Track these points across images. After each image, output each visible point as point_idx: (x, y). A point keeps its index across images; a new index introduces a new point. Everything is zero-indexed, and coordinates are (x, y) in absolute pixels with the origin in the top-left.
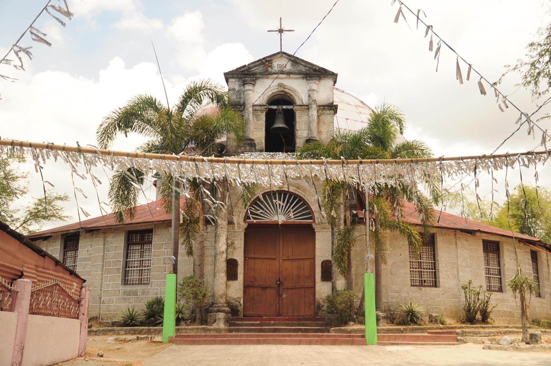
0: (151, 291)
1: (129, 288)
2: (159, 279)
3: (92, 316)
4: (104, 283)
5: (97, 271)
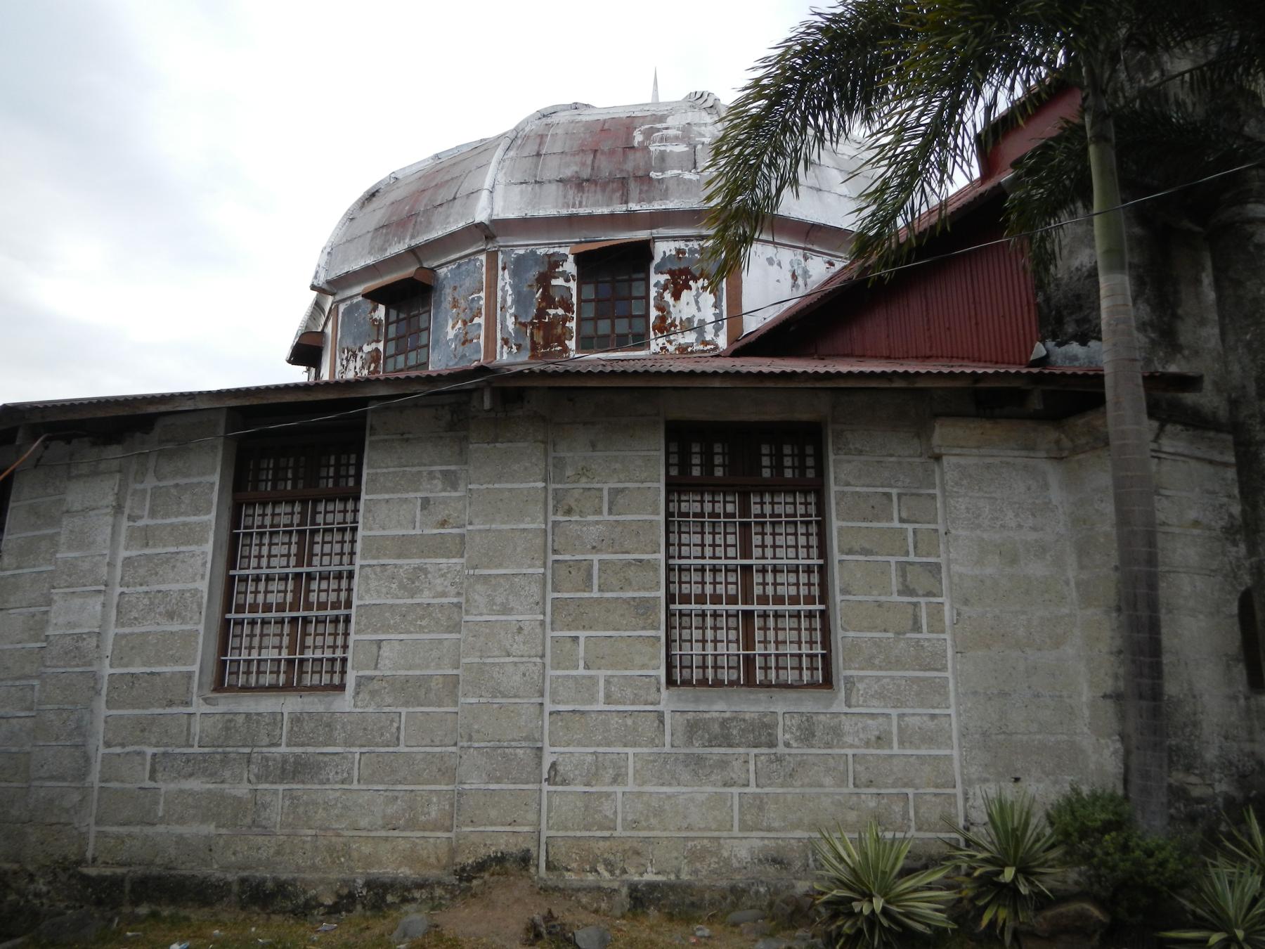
0: (847, 724)
1: (718, 706)
2: (889, 664)
3: (482, 852)
4: (550, 672)
5: (506, 610)
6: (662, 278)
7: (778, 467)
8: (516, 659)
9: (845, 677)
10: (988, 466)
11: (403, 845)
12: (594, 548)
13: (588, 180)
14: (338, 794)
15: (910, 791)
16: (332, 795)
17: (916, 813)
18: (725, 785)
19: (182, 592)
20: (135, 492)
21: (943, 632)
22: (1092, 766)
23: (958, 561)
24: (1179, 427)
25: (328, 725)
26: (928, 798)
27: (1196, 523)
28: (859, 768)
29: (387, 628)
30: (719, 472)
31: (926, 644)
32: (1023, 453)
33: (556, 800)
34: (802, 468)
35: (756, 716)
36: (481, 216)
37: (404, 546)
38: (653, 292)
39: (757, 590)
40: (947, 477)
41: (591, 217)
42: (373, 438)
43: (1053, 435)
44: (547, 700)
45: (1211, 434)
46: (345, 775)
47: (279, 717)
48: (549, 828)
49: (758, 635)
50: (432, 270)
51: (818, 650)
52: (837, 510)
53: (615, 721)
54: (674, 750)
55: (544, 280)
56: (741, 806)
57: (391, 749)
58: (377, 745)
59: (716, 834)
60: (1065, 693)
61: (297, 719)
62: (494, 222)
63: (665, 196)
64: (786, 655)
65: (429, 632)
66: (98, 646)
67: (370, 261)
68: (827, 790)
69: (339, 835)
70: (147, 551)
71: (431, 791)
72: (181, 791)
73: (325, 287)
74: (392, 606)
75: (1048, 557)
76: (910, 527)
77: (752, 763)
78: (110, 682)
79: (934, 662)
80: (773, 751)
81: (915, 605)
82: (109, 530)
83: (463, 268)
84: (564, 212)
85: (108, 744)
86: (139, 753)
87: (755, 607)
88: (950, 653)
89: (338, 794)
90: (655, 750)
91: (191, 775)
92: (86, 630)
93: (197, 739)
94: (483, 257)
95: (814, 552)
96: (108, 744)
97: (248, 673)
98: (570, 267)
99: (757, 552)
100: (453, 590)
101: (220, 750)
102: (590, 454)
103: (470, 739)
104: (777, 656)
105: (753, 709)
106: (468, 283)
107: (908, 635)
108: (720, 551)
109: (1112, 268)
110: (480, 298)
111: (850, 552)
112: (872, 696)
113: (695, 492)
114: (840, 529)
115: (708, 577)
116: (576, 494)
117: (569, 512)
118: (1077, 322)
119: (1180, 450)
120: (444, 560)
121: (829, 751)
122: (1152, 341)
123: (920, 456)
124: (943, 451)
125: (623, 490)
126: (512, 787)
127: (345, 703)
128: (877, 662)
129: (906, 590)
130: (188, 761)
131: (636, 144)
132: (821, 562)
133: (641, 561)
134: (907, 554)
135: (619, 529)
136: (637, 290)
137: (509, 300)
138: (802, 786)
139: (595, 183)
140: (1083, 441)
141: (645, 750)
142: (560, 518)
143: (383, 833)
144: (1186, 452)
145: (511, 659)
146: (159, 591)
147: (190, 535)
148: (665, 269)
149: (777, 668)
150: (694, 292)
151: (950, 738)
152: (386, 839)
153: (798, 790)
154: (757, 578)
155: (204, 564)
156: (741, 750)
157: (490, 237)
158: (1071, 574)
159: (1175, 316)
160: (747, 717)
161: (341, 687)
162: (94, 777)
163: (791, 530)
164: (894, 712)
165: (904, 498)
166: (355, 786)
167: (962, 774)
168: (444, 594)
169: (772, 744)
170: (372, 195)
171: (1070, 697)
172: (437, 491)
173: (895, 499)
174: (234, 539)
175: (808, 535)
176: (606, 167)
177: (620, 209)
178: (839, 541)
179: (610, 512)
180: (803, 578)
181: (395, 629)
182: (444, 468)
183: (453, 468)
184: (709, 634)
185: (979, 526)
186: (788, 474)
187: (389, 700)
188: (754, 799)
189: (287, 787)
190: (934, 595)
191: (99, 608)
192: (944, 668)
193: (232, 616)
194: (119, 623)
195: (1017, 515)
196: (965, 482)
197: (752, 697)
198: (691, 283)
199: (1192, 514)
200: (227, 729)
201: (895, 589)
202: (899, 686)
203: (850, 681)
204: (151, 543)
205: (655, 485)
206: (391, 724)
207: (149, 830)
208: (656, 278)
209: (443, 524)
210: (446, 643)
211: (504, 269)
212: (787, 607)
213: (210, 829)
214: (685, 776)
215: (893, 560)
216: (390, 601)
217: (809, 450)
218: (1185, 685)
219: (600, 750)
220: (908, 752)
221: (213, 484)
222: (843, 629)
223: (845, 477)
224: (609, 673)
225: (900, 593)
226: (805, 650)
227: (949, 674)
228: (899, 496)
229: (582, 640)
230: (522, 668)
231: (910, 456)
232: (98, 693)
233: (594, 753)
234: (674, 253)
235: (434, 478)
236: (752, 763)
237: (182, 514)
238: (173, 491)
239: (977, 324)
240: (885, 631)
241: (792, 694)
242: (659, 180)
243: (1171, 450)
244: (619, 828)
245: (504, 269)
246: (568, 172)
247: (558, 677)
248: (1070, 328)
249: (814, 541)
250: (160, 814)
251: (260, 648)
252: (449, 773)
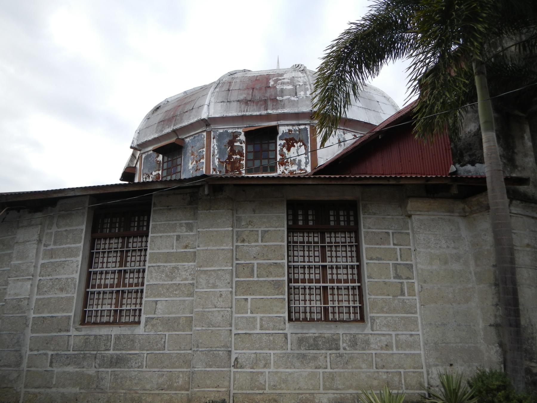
0: (372, 339)
1: (312, 331)
4: (235, 315)
5: (214, 286)
6: (283, 142)
7: (338, 221)
8: (219, 309)
9: (370, 317)
10: (433, 220)
11: (166, 397)
12: (255, 257)
13: (250, 101)
14: (136, 373)
15: (402, 371)
16: (134, 374)
17: (405, 381)
18: (316, 368)
19: (67, 279)
20: (47, 234)
21: (415, 295)
22: (486, 359)
23: (421, 263)
24: (519, 202)
25: (132, 340)
26: (410, 374)
27: (528, 245)
28: (378, 360)
29: (160, 295)
30: (311, 223)
31: (407, 301)
32: (448, 214)
33: (238, 376)
34: (349, 221)
35: (330, 335)
36: (204, 116)
37: (168, 257)
38: (278, 148)
39: (329, 277)
40: (414, 225)
41: (251, 116)
42: (155, 208)
43: (461, 206)
44: (233, 329)
45: (533, 205)
46: (140, 364)
47: (110, 337)
48: (234, 389)
49: (330, 298)
50: (183, 139)
51: (358, 304)
52: (365, 240)
53: (265, 338)
54: (292, 352)
55: (231, 143)
56: (324, 378)
57: (161, 352)
58: (155, 350)
59: (312, 391)
60: (472, 324)
61: (118, 338)
62: (209, 118)
63: (283, 107)
64: (343, 307)
65: (179, 297)
66: (28, 304)
67: (156, 136)
68: (363, 370)
69: (137, 393)
70: (52, 260)
71: (180, 372)
72: (64, 372)
73: (137, 147)
74: (162, 284)
75: (461, 261)
76: (398, 247)
77: (328, 357)
78: (33, 320)
79: (411, 310)
80: (338, 352)
81: (402, 283)
82: (35, 251)
83: (196, 138)
84: (240, 114)
85: (31, 350)
86: (45, 354)
87: (328, 284)
88: (418, 305)
89: (136, 373)
90: (284, 351)
91: (69, 364)
92: (23, 297)
93: (72, 347)
94: (205, 134)
95: (355, 259)
96: (31, 350)
97: (96, 316)
98: (242, 137)
99: (329, 259)
100: (190, 277)
101: (82, 352)
102: (253, 215)
103: (198, 347)
104: (339, 307)
105: (328, 332)
106: (198, 145)
107: (399, 297)
108: (312, 259)
109: (487, 130)
110: (203, 151)
111: (371, 259)
112: (383, 326)
113: (300, 232)
114: (366, 248)
115: (307, 271)
116: (246, 233)
117: (243, 241)
118: (470, 155)
119: (519, 212)
120: (187, 264)
121: (364, 352)
122: (504, 164)
123: (402, 215)
124: (412, 213)
125: (268, 231)
126: (217, 369)
127: (140, 330)
128: (385, 310)
129: (397, 276)
130: (68, 358)
131: (271, 86)
132: (358, 264)
133: (276, 263)
134: (397, 260)
135: (266, 249)
136: (272, 147)
137: (216, 152)
138: (352, 368)
139: (253, 102)
140: (475, 208)
141: (279, 352)
142: (239, 244)
143: (157, 392)
144: (522, 213)
145: (217, 309)
146: (57, 279)
147: (72, 253)
148: (283, 138)
149: (339, 313)
150: (296, 148)
151: (420, 345)
152: (158, 394)
153: (350, 371)
154: (329, 271)
155: (77, 266)
156: (323, 351)
157: (208, 125)
158: (472, 268)
159: (513, 152)
160: (326, 336)
161: (139, 323)
162: (24, 365)
163: (344, 249)
164: (393, 333)
165: (395, 235)
166: (144, 369)
167: (426, 362)
168: (186, 279)
169: (338, 349)
170: (157, 108)
171: (474, 326)
172: (183, 232)
173: (391, 235)
174: (91, 255)
175: (351, 251)
176: (258, 95)
177: (264, 112)
178: (366, 254)
179: (262, 241)
180: (350, 271)
181: (164, 295)
182: (187, 221)
183: (191, 221)
184: (308, 297)
185: (430, 247)
186: (342, 224)
187: (160, 329)
188: (330, 375)
189: (113, 370)
190: (410, 279)
191: (29, 286)
192: (416, 313)
193: (90, 290)
194: (38, 293)
195: (446, 242)
196: (422, 227)
197: (328, 326)
198: (295, 144)
199: (526, 241)
200: (86, 342)
201: (392, 276)
202: (395, 321)
203: (373, 319)
204: (54, 256)
205: (283, 229)
206: (161, 340)
207: (48, 390)
208: (279, 142)
209: (186, 247)
210: (187, 302)
211: (214, 138)
212: (343, 284)
213: (77, 390)
214: (298, 364)
215: (391, 262)
216: (161, 283)
217: (351, 213)
218: (527, 320)
219: (258, 351)
220: (400, 352)
221: (82, 230)
222: (369, 294)
223: (368, 225)
224: (262, 315)
225: (394, 278)
226: (351, 304)
227: (418, 315)
228: (393, 233)
229: (249, 300)
230: (222, 313)
231: (397, 215)
232: (28, 326)
233: (255, 353)
234: (287, 131)
235: (182, 226)
236: (328, 357)
237: (68, 243)
238: (65, 233)
239: (422, 158)
240: (388, 295)
241: (346, 325)
242: (280, 101)
243: (515, 212)
244: (267, 389)
245: (214, 138)
246: (241, 97)
247: (238, 317)
248: (467, 159)
249: (354, 254)
250: (54, 383)
251: (102, 305)
252: (188, 363)
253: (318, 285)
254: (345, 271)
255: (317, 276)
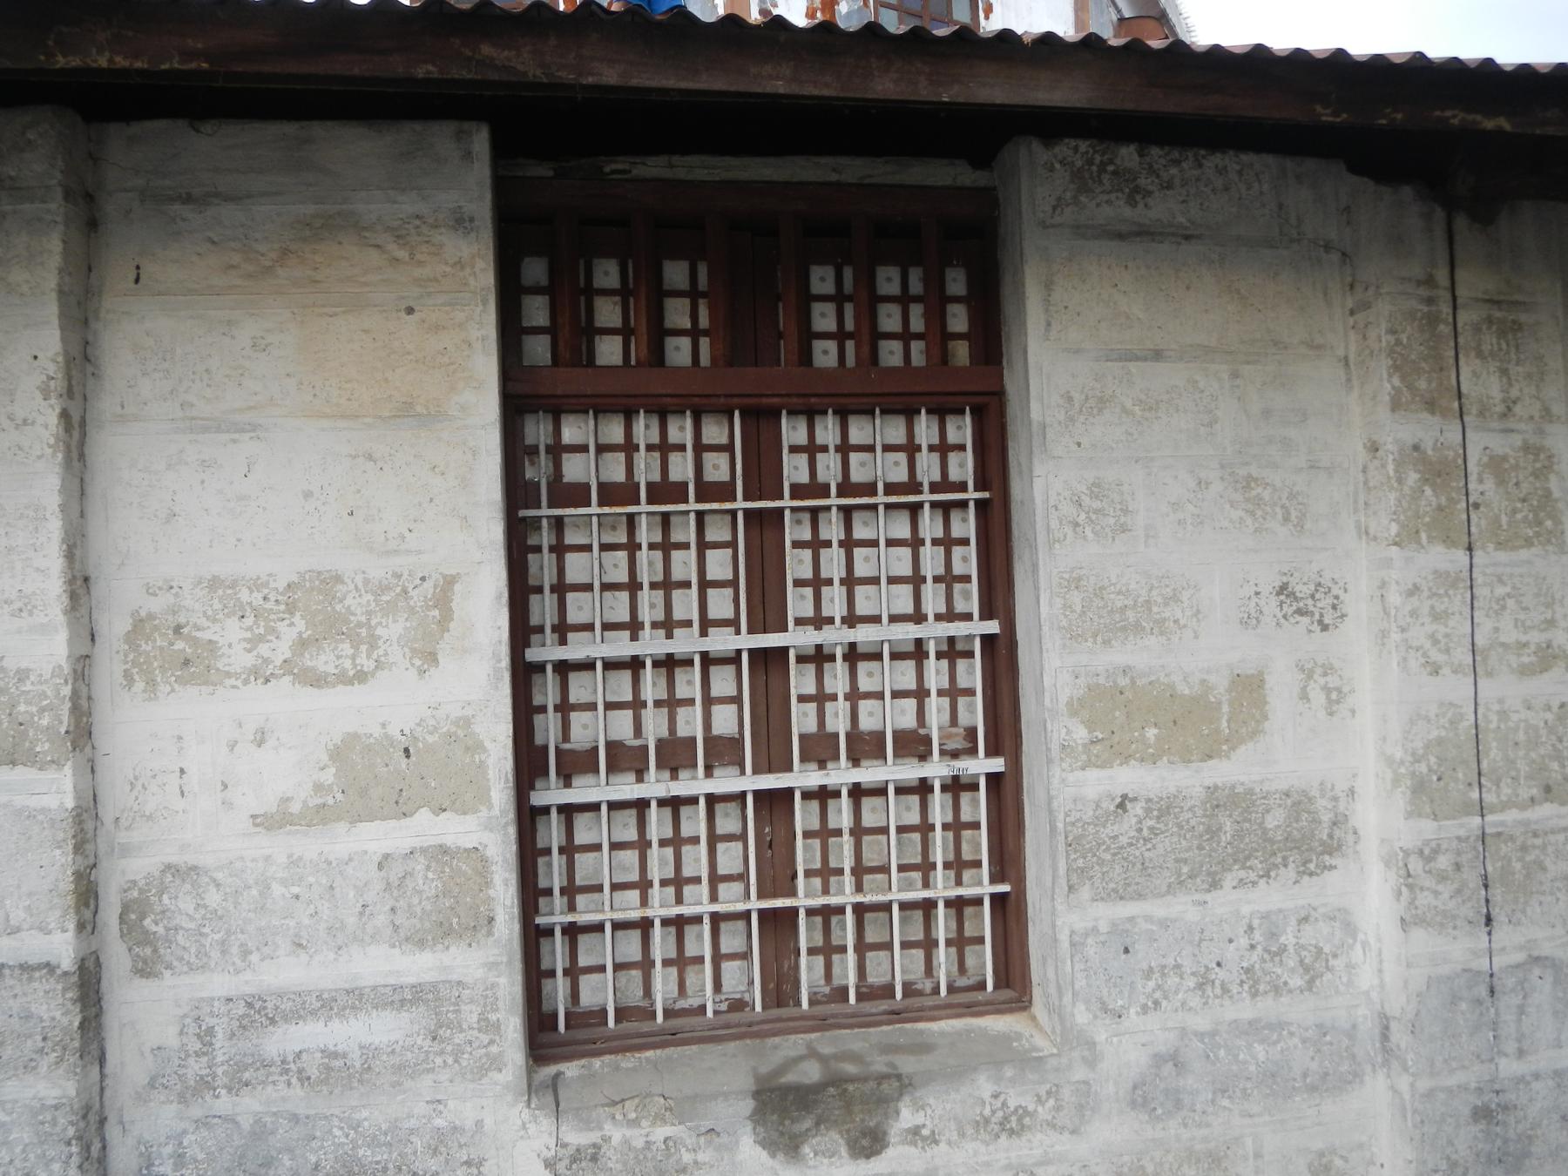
30: (679, 352)
39: (803, 720)
49: (805, 855)
51: (982, 885)
95: (969, 598)
99: (798, 603)
104: (860, 909)
115: (652, 686)
149: (862, 947)
154: (801, 680)
175: (947, 543)
226: (942, 888)
249: (967, 561)
253: (726, 782)
254: (905, 674)
255: (725, 721)
